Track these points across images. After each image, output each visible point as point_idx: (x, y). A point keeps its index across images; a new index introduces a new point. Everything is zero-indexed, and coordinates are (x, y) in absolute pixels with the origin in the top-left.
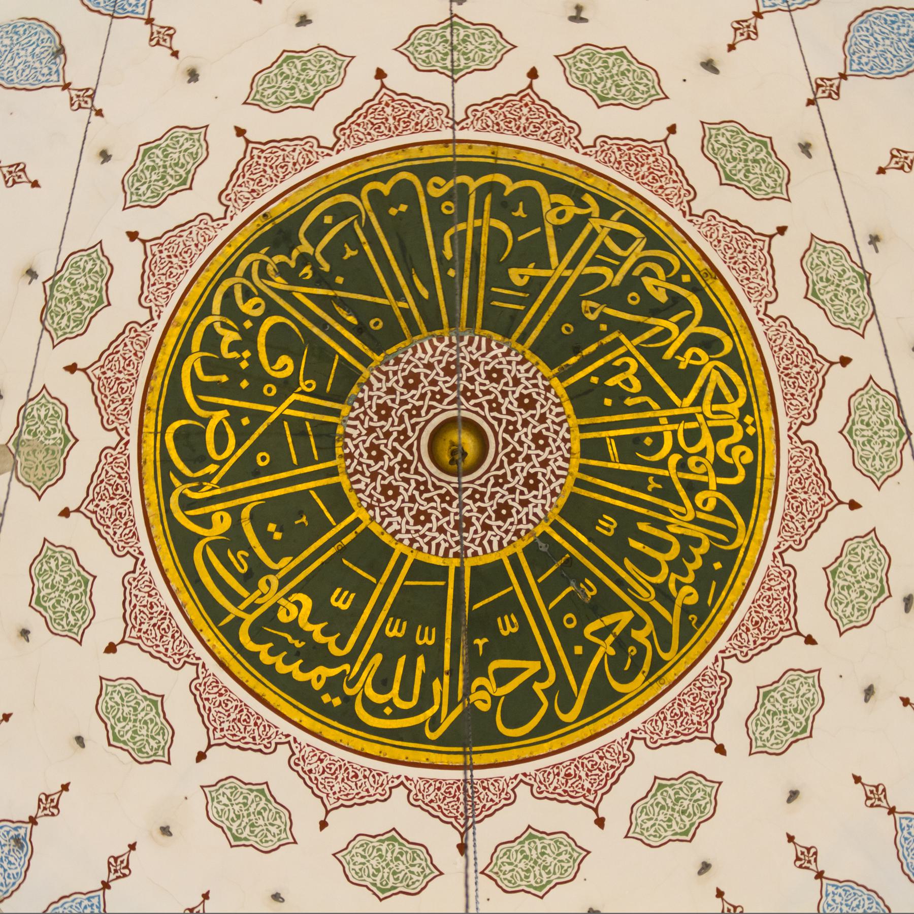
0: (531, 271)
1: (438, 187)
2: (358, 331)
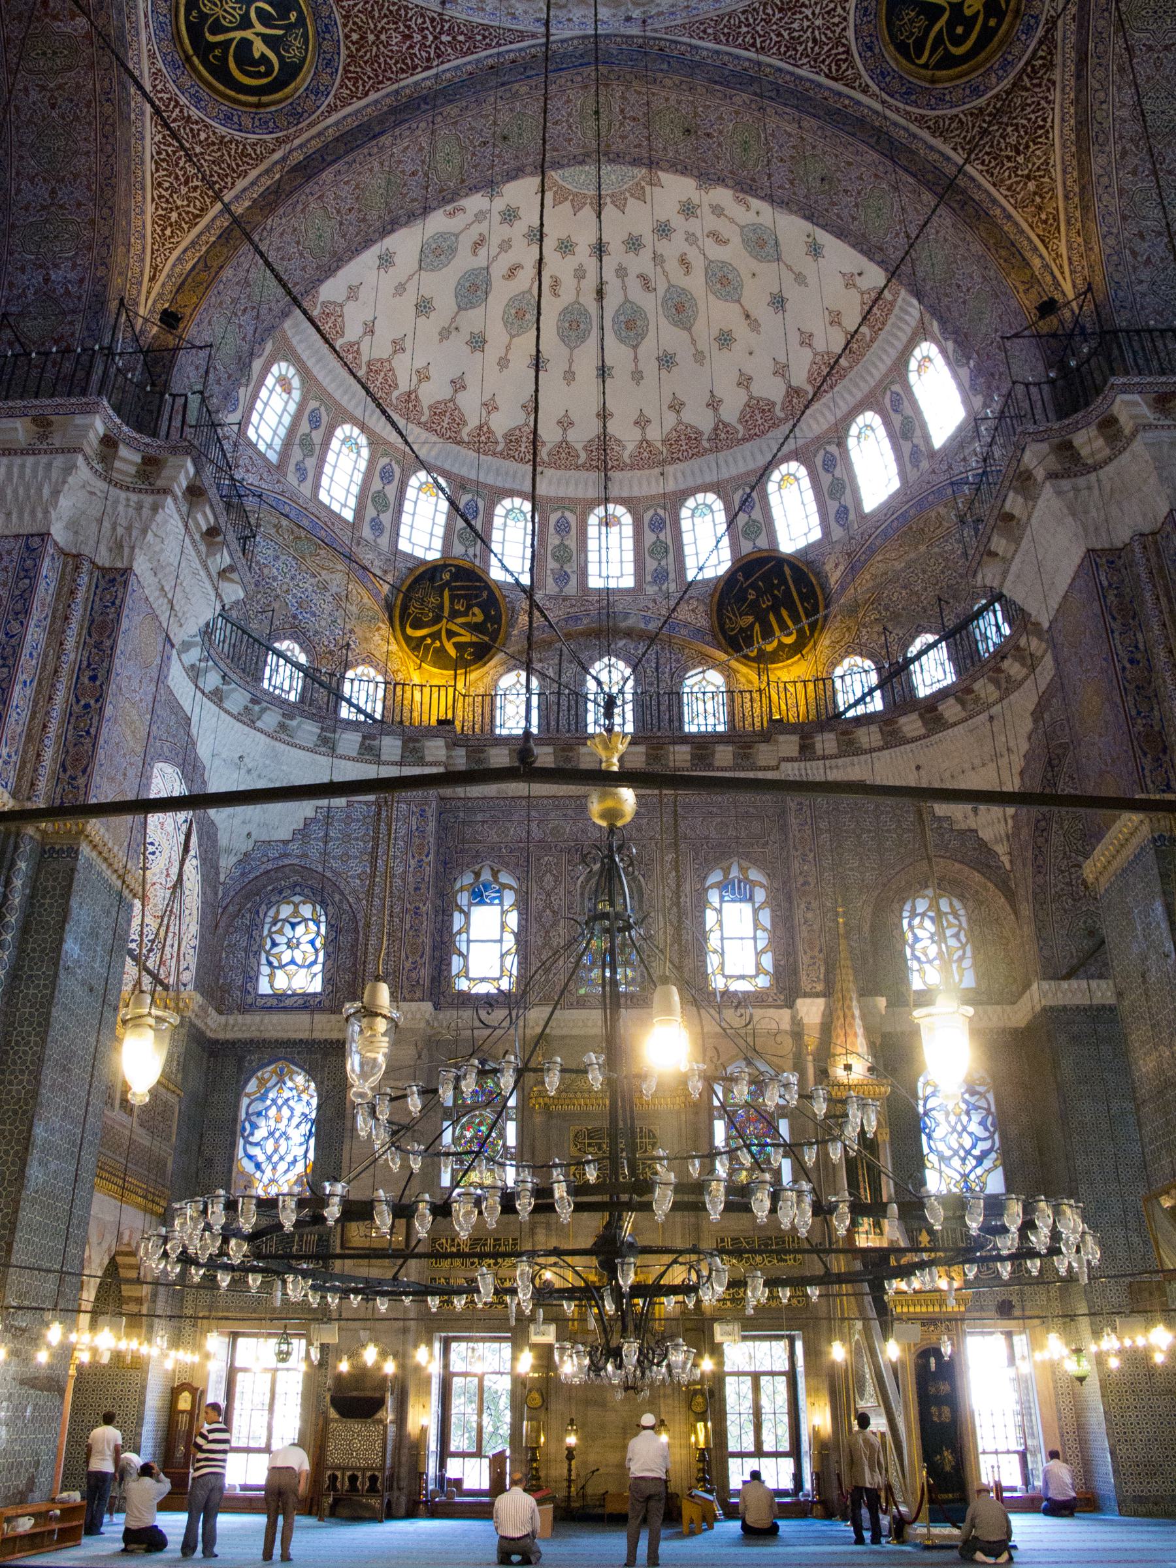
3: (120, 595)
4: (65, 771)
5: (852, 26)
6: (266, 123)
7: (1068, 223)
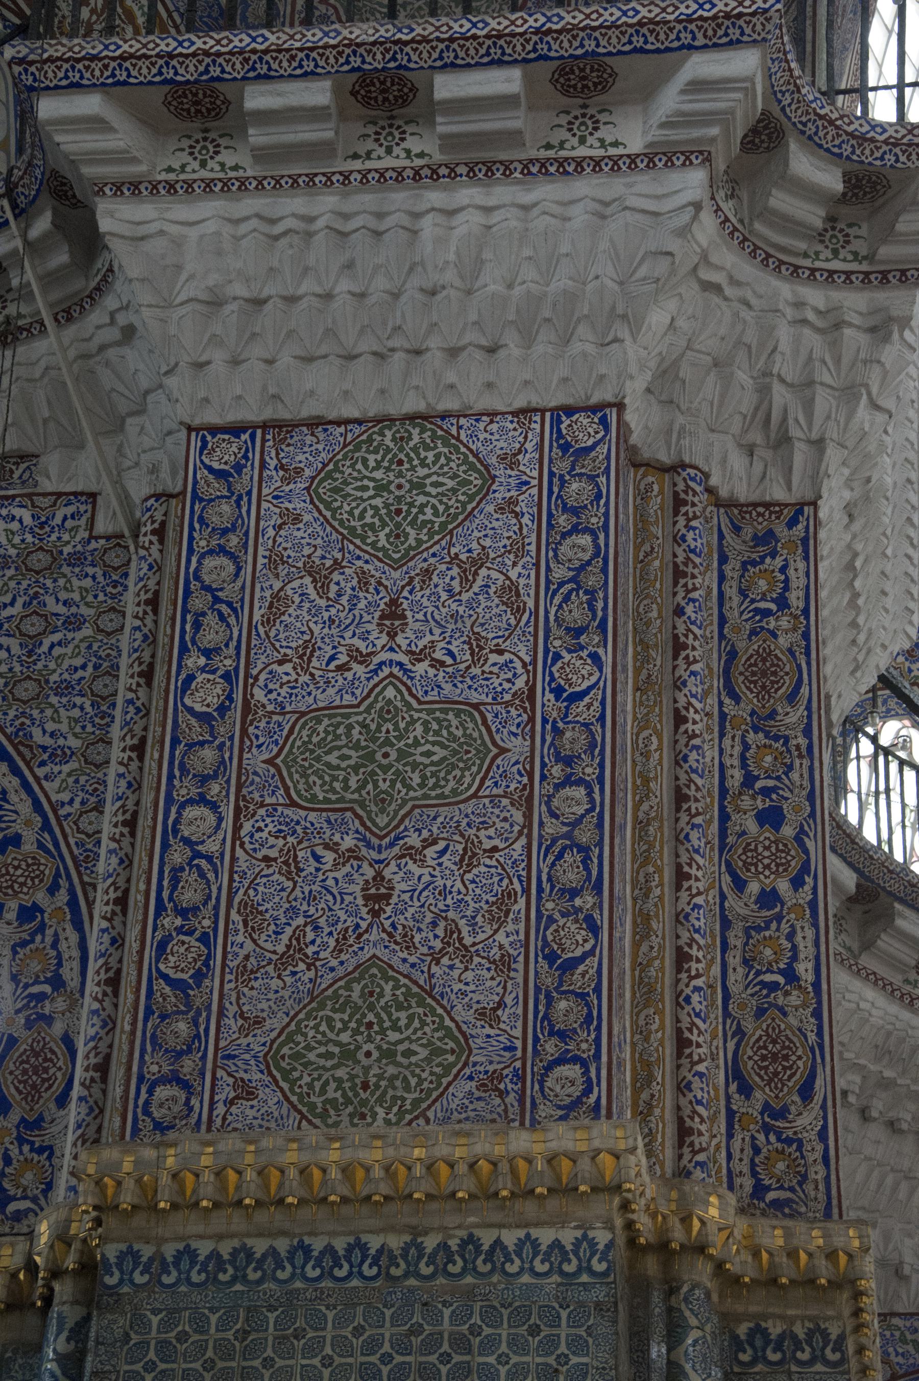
3: (797, 580)
4: (746, 1090)
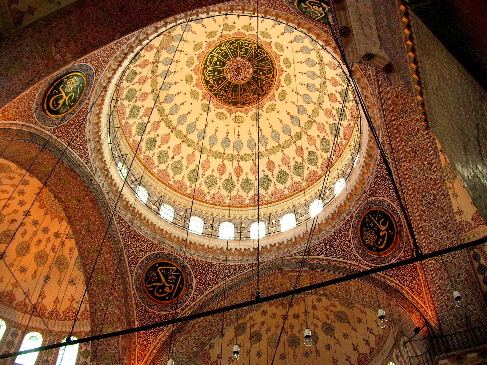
0: (262, 74)
1: (269, 63)
2: (250, 57)
5: (143, 259)
6: (40, 115)
7: (146, 361)
